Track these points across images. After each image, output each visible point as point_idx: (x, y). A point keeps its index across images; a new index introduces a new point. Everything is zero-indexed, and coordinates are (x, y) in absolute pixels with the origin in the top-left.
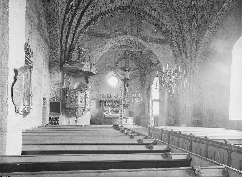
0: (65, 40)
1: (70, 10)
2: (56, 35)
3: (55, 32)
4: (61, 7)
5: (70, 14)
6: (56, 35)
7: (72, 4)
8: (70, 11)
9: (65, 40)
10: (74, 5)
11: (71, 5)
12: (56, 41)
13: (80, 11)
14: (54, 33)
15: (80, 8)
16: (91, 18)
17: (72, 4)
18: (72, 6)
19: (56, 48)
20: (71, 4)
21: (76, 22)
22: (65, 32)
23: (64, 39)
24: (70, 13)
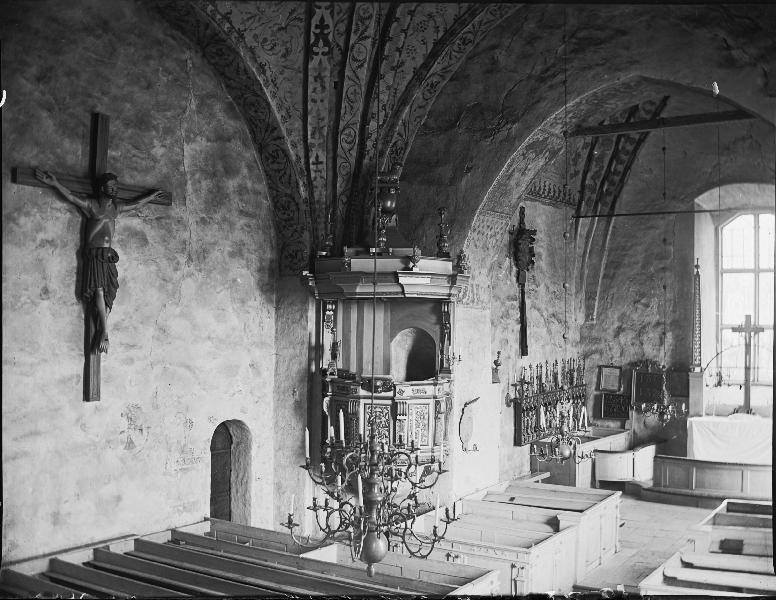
0: (321, 163)
1: (316, 44)
2: (280, 153)
3: (274, 142)
4: (277, 48)
5: (325, 59)
6: (280, 153)
7: (322, 20)
8: (321, 48)
9: (321, 163)
10: (329, 21)
11: (317, 27)
12: (286, 177)
13: (365, 30)
14: (275, 148)
15: (362, 20)
16: (441, 29)
17: (322, 20)
18: (322, 25)
19: (289, 202)
20: (315, 21)
21: (364, 74)
22: (318, 130)
23: (317, 157)
24: (323, 54)
